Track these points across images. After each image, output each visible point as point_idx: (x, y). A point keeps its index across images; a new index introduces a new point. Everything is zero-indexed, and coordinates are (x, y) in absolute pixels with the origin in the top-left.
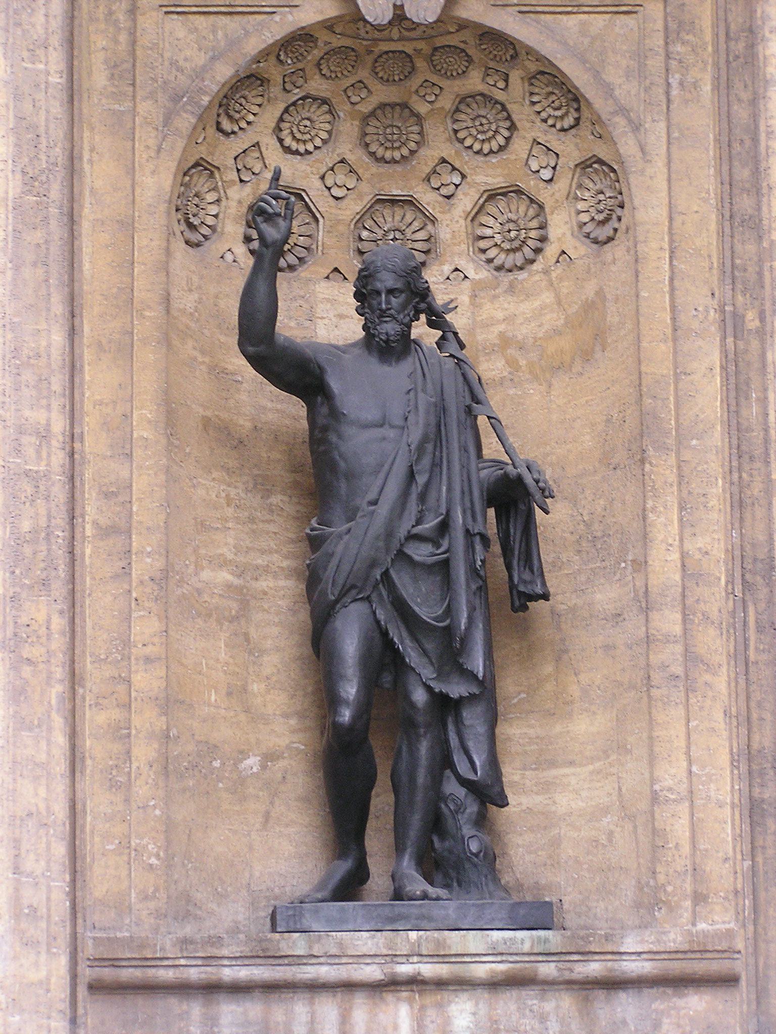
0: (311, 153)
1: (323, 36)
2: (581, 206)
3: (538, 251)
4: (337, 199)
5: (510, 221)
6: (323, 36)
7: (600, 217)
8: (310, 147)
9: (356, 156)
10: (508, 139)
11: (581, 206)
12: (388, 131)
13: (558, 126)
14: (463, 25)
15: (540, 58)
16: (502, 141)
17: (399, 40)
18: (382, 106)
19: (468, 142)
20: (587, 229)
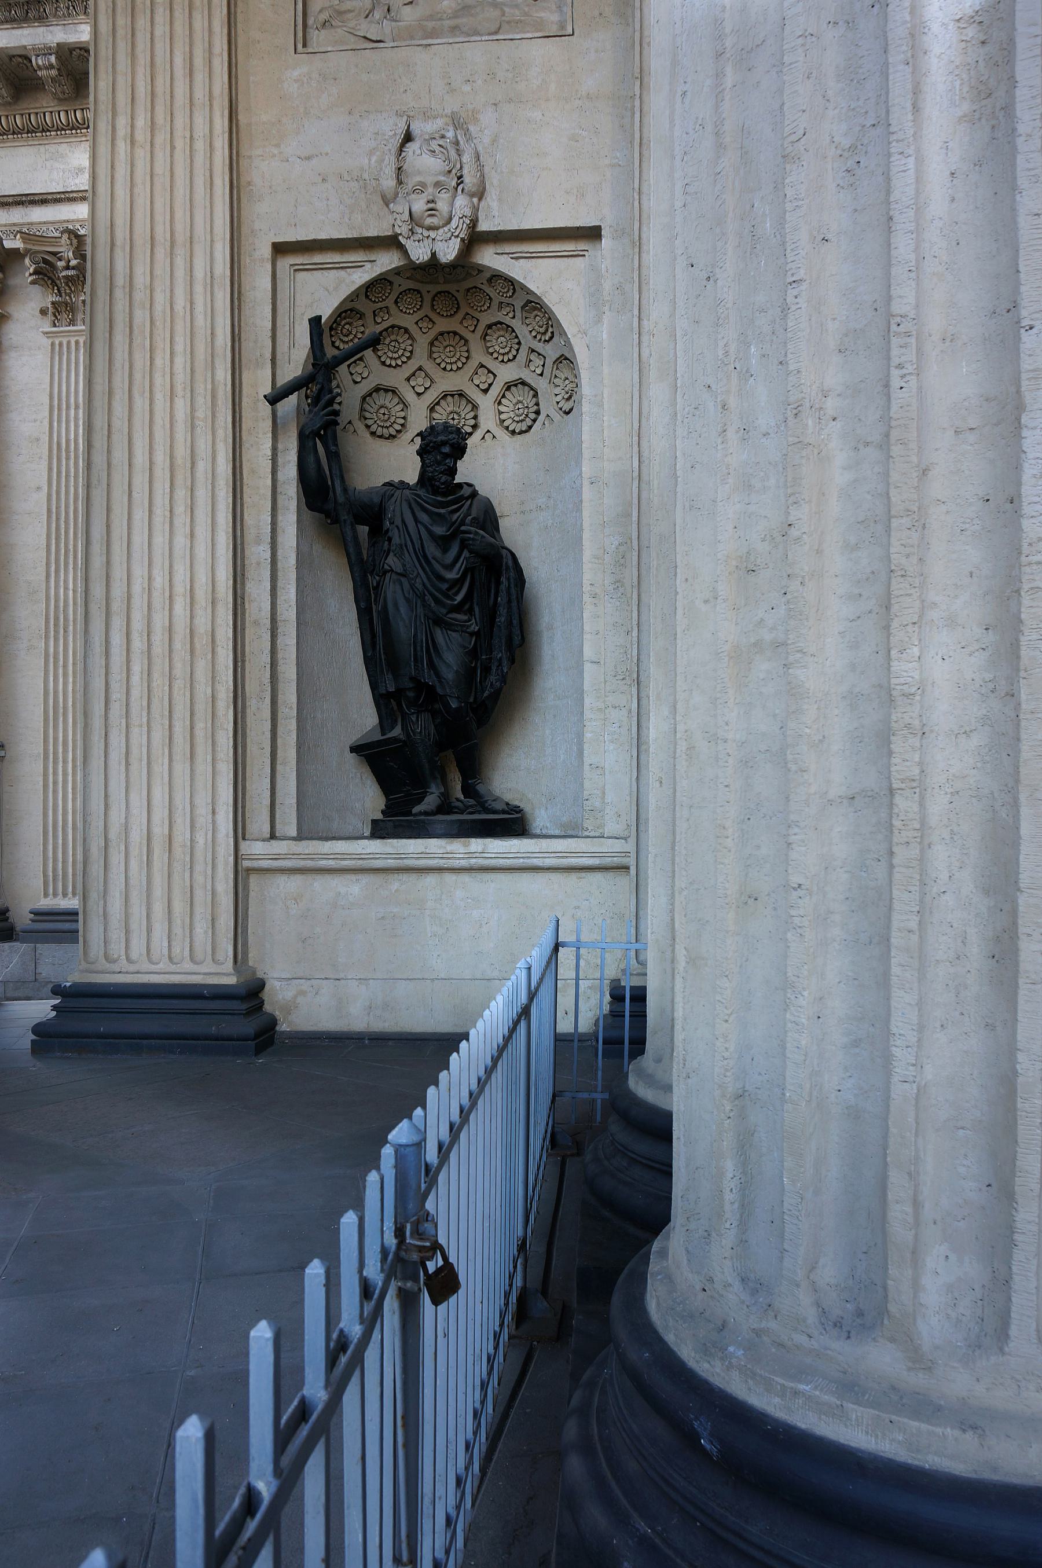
0: (400, 366)
1: (397, 280)
2: (557, 391)
3: (534, 421)
4: (419, 394)
5: (521, 402)
6: (397, 280)
7: (566, 396)
8: (399, 362)
9: (429, 366)
10: (518, 350)
11: (557, 391)
12: (448, 350)
13: (543, 339)
14: (480, 269)
15: (529, 292)
16: (515, 353)
17: (444, 283)
18: (442, 334)
19: (495, 355)
20: (560, 405)
